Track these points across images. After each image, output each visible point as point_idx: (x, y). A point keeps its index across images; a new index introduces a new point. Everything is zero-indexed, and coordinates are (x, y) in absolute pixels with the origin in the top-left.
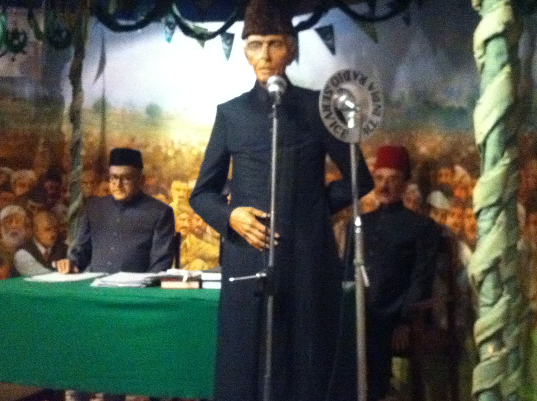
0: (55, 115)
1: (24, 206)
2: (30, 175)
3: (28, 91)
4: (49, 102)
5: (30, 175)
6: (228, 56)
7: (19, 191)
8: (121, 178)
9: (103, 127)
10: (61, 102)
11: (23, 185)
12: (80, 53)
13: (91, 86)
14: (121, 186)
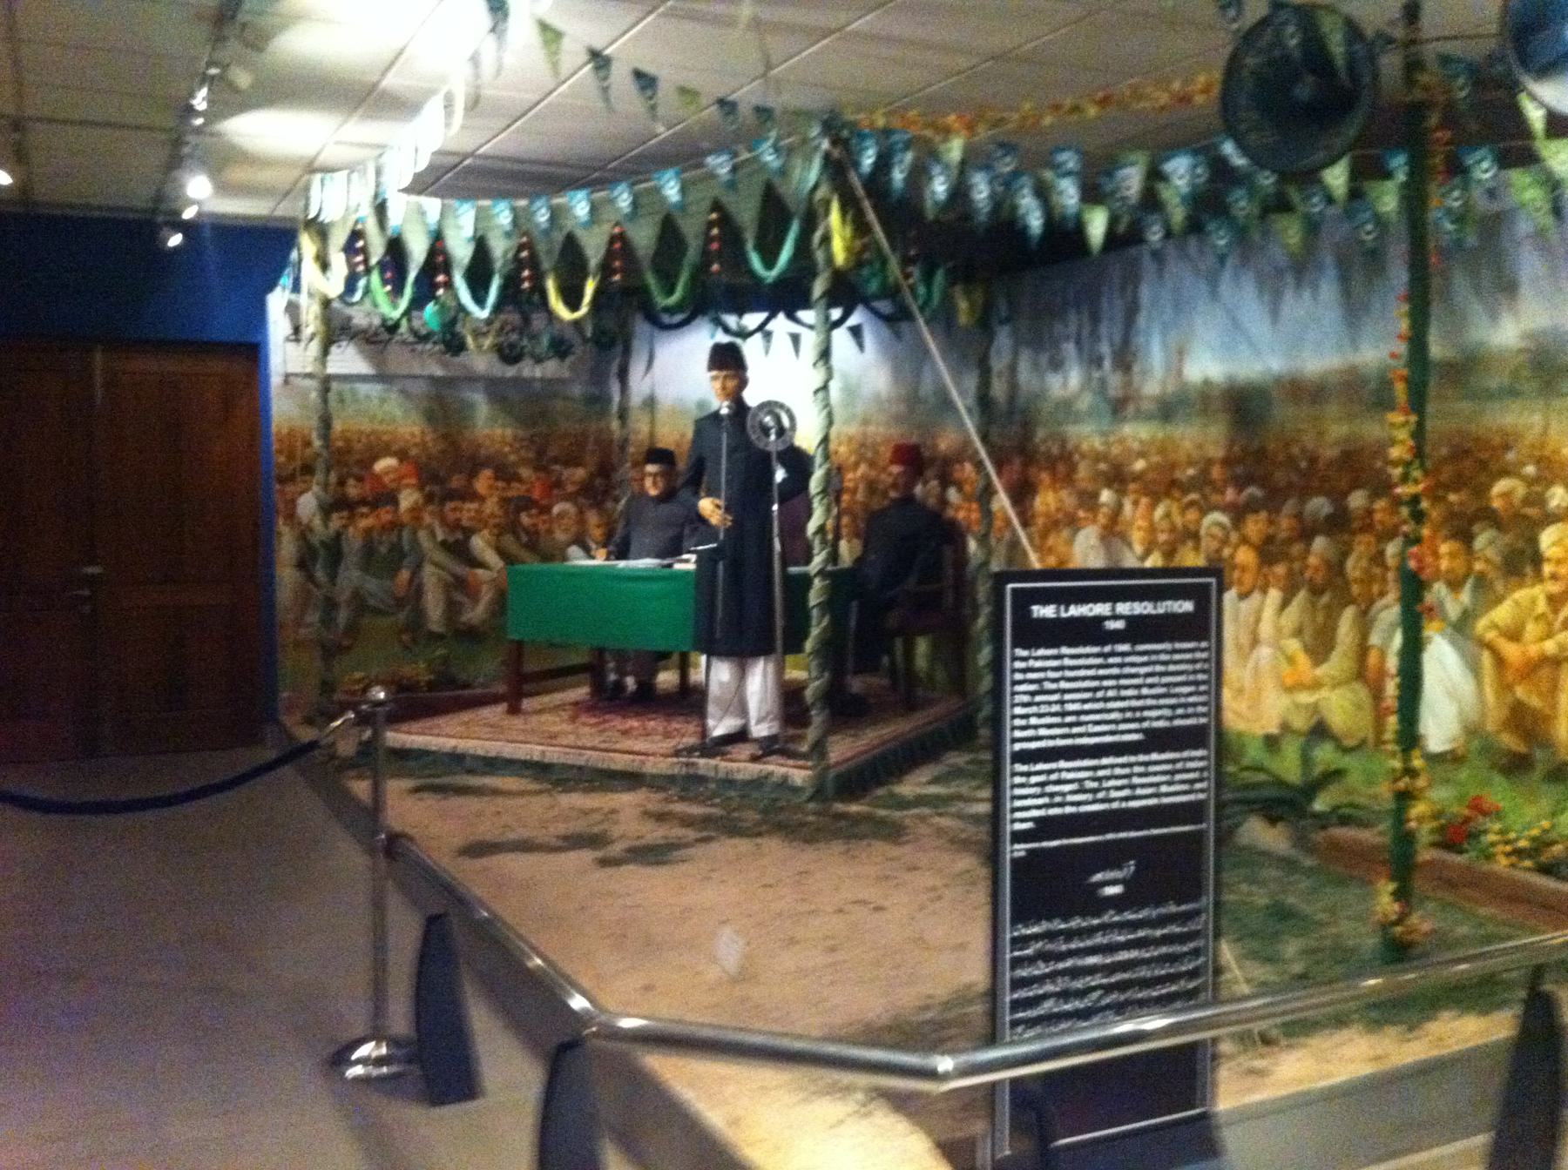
0: (604, 413)
1: (576, 504)
2: (580, 473)
3: (577, 390)
4: (598, 401)
5: (580, 473)
6: (767, 352)
7: (570, 488)
8: (655, 475)
9: (652, 422)
10: (609, 400)
11: (573, 483)
12: (627, 352)
13: (639, 385)
14: (655, 484)
